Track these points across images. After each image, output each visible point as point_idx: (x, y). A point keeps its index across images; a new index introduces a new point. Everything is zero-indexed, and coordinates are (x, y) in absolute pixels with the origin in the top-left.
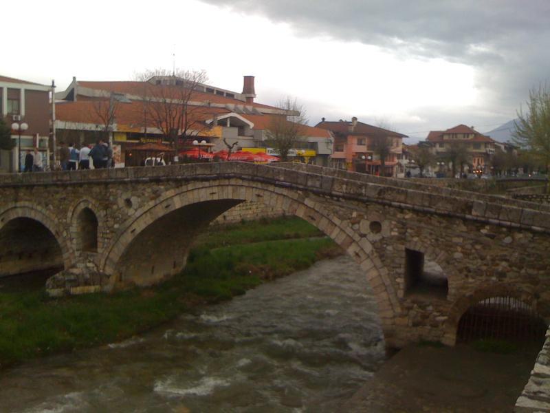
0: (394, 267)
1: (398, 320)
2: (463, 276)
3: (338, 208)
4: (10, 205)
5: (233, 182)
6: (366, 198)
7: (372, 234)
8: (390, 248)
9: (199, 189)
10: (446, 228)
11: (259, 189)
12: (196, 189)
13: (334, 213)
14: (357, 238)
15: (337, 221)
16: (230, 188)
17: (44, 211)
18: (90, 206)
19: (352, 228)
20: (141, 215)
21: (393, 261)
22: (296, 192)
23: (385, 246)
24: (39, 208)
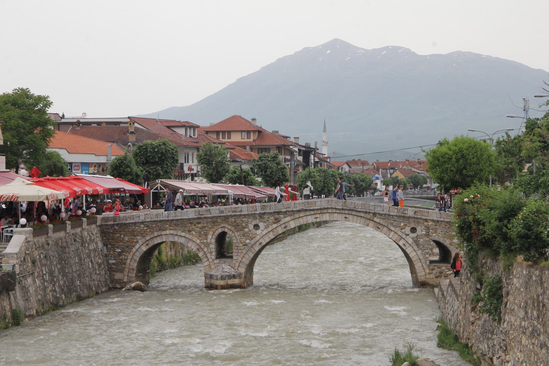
1: (428, 276)
3: (393, 221)
4: (156, 234)
5: (330, 211)
6: (408, 215)
7: (412, 234)
8: (421, 240)
9: (306, 216)
10: (449, 228)
11: (346, 214)
14: (404, 236)
15: (392, 228)
16: (328, 214)
17: (187, 236)
20: (266, 234)
24: (183, 234)
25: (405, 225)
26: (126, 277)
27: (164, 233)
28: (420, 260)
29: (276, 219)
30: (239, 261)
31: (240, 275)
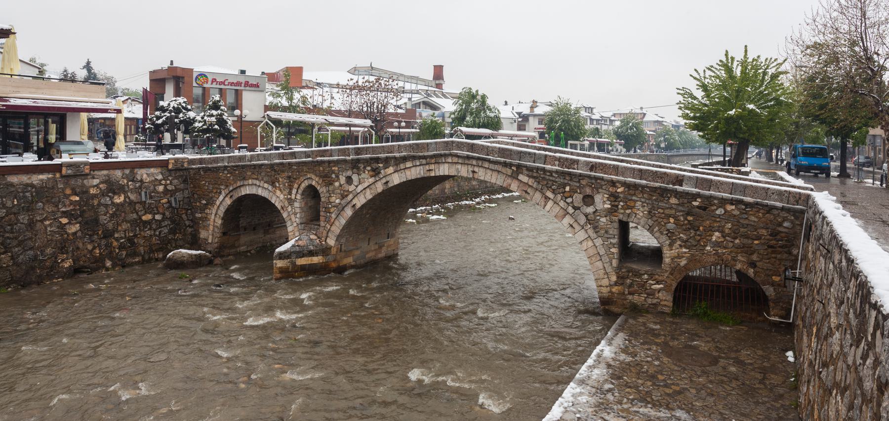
0: (608, 238)
2: (678, 247)
4: (239, 184)
5: (450, 160)
11: (474, 165)
12: (414, 166)
13: (547, 187)
15: (550, 194)
16: (446, 165)
18: (314, 183)
19: (565, 201)
20: (361, 191)
21: (606, 232)
22: (511, 168)
23: (598, 218)
24: (266, 185)
25: (574, 191)
26: (211, 237)
27: (246, 183)
28: (600, 256)
29: (373, 170)
30: (327, 230)
31: (325, 251)
